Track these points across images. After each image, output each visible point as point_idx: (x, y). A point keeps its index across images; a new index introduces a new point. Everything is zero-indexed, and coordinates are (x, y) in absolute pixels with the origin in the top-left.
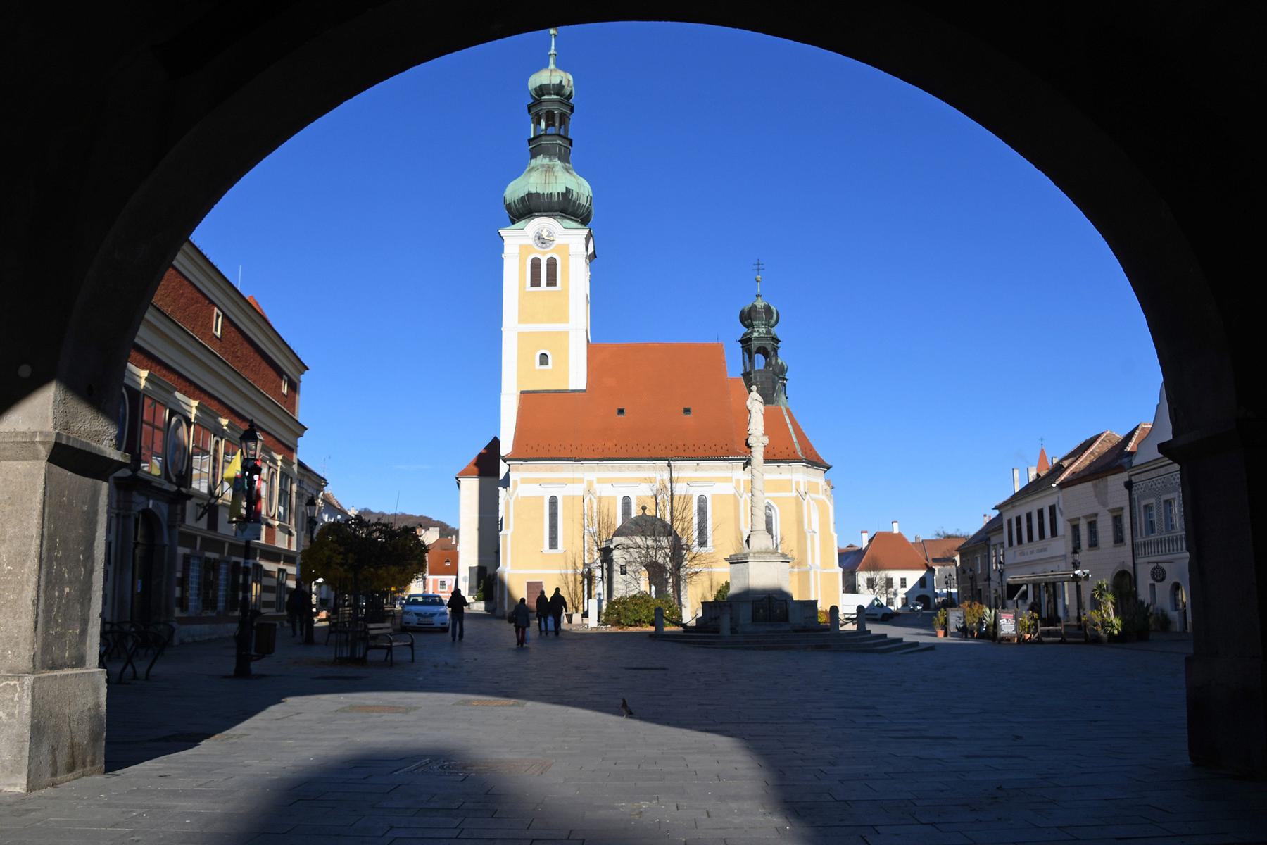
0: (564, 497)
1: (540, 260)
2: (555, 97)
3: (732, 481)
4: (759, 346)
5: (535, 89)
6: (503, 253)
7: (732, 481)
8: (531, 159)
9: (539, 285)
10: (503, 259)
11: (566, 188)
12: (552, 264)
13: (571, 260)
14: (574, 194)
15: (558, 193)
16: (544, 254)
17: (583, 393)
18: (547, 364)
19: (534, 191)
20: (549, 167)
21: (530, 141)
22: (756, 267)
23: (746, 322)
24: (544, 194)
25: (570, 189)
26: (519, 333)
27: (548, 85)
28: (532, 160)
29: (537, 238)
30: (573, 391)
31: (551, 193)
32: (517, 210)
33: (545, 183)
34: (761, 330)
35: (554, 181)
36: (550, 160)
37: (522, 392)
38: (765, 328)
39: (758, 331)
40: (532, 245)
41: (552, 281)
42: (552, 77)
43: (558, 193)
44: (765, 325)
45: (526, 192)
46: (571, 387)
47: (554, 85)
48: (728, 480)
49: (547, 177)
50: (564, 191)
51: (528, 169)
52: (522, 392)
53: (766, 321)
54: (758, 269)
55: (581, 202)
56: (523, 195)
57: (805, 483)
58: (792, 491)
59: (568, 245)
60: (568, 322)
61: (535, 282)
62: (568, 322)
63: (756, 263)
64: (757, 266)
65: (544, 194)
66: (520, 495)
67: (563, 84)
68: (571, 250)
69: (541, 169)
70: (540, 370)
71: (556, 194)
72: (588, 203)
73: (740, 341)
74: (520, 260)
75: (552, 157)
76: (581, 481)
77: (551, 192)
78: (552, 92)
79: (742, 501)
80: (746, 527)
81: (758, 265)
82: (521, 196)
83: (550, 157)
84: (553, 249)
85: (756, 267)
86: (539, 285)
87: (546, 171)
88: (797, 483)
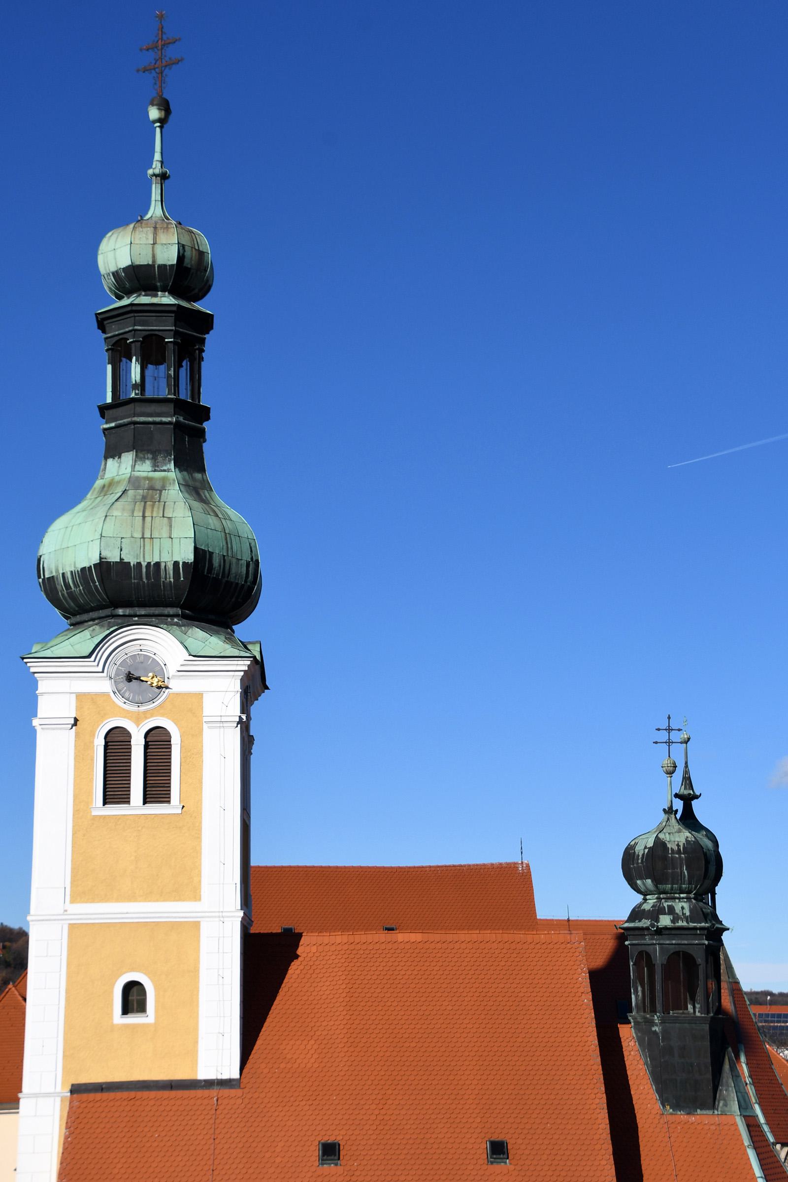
1: (129, 735)
2: (167, 299)
4: (672, 949)
5: (116, 274)
6: (36, 716)
8: (106, 458)
9: (124, 798)
10: (34, 731)
14: (216, 562)
15: (176, 564)
16: (138, 719)
17: (233, 1092)
19: (113, 556)
20: (152, 488)
21: (103, 410)
22: (664, 736)
23: (639, 882)
24: (139, 564)
27: (148, 265)
28: (110, 461)
29: (122, 677)
30: (209, 1084)
31: (158, 564)
32: (71, 595)
33: (143, 538)
34: (678, 906)
35: (165, 534)
36: (155, 468)
37: (76, 1090)
38: (689, 899)
39: (671, 910)
42: (158, 248)
43: (176, 564)
44: (689, 892)
45: (95, 560)
46: (204, 1073)
47: (162, 267)
49: (148, 520)
50: (190, 557)
51: (99, 483)
52: (76, 1090)
53: (690, 883)
54: (669, 743)
55: (232, 578)
56: (87, 565)
59: (199, 696)
60: (196, 896)
62: (196, 896)
63: (665, 726)
64: (666, 733)
65: (139, 564)
67: (187, 262)
69: (131, 493)
71: (170, 567)
72: (251, 578)
74: (77, 735)
75: (160, 459)
77: (156, 559)
78: (159, 284)
81: (669, 730)
82: (80, 566)
83: (154, 459)
84: (160, 706)
85: (664, 736)
86: (124, 798)
87: (144, 499)
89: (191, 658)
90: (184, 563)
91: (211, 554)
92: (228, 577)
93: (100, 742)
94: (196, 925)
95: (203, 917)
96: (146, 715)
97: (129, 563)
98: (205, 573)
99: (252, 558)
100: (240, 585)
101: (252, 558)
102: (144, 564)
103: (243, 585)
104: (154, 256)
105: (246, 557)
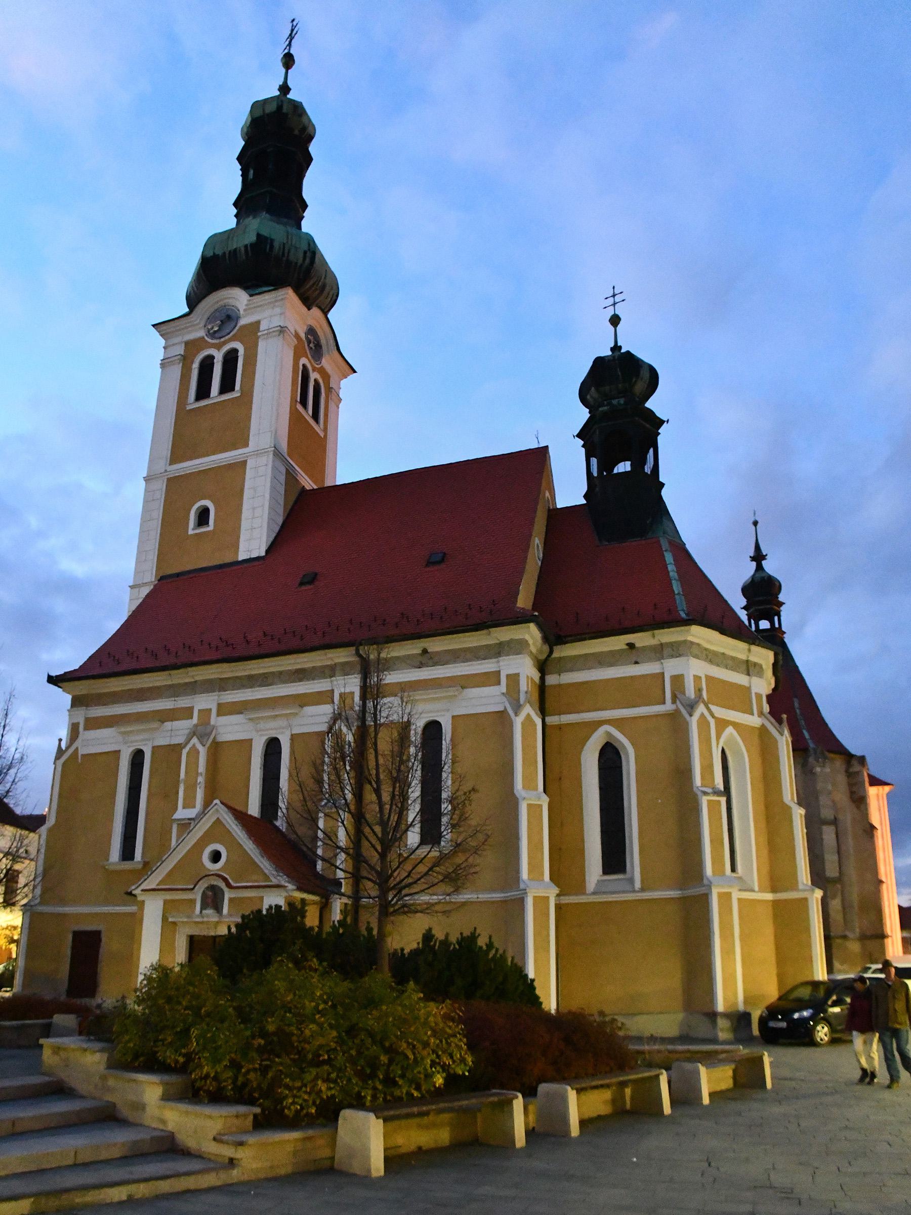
0: (155, 749)
3: (498, 683)
7: (499, 683)
11: (259, 235)
12: (231, 359)
13: (262, 345)
14: (276, 245)
16: (218, 347)
18: (207, 523)
24: (224, 253)
25: (266, 238)
26: (169, 480)
31: (235, 249)
37: (162, 579)
40: (203, 338)
41: (227, 385)
43: (246, 246)
47: (268, 115)
48: (492, 678)
55: (292, 258)
57: (697, 678)
58: (664, 703)
61: (203, 392)
62: (246, 445)
66: (81, 752)
67: (285, 110)
68: (263, 326)
70: (196, 534)
71: (243, 249)
72: (308, 261)
73: (579, 436)
76: (187, 713)
79: (518, 722)
80: (529, 784)
84: (234, 336)
88: (678, 680)
89: (252, 298)
90: (251, 245)
91: (272, 241)
92: (288, 256)
93: (196, 366)
94: (245, 463)
95: (247, 457)
96: (225, 343)
97: (218, 255)
98: (268, 250)
99: (309, 250)
100: (299, 264)
101: (309, 250)
102: (227, 253)
103: (301, 265)
104: (264, 110)
105: (304, 247)
